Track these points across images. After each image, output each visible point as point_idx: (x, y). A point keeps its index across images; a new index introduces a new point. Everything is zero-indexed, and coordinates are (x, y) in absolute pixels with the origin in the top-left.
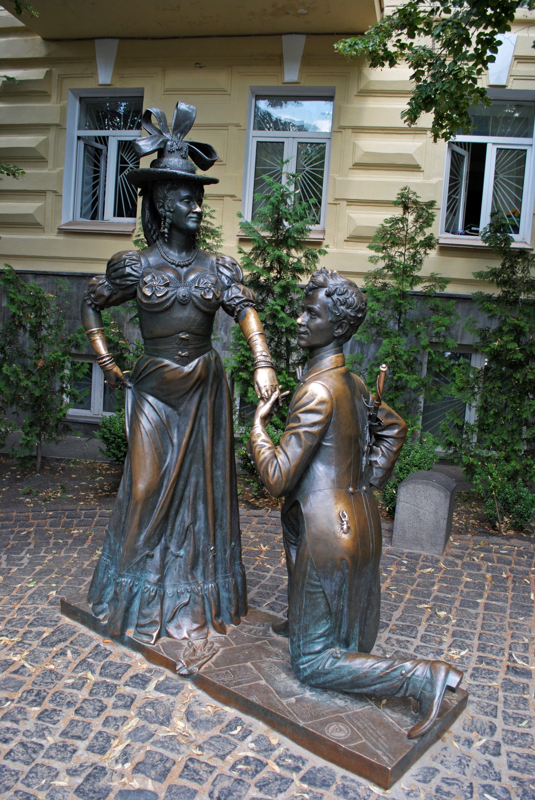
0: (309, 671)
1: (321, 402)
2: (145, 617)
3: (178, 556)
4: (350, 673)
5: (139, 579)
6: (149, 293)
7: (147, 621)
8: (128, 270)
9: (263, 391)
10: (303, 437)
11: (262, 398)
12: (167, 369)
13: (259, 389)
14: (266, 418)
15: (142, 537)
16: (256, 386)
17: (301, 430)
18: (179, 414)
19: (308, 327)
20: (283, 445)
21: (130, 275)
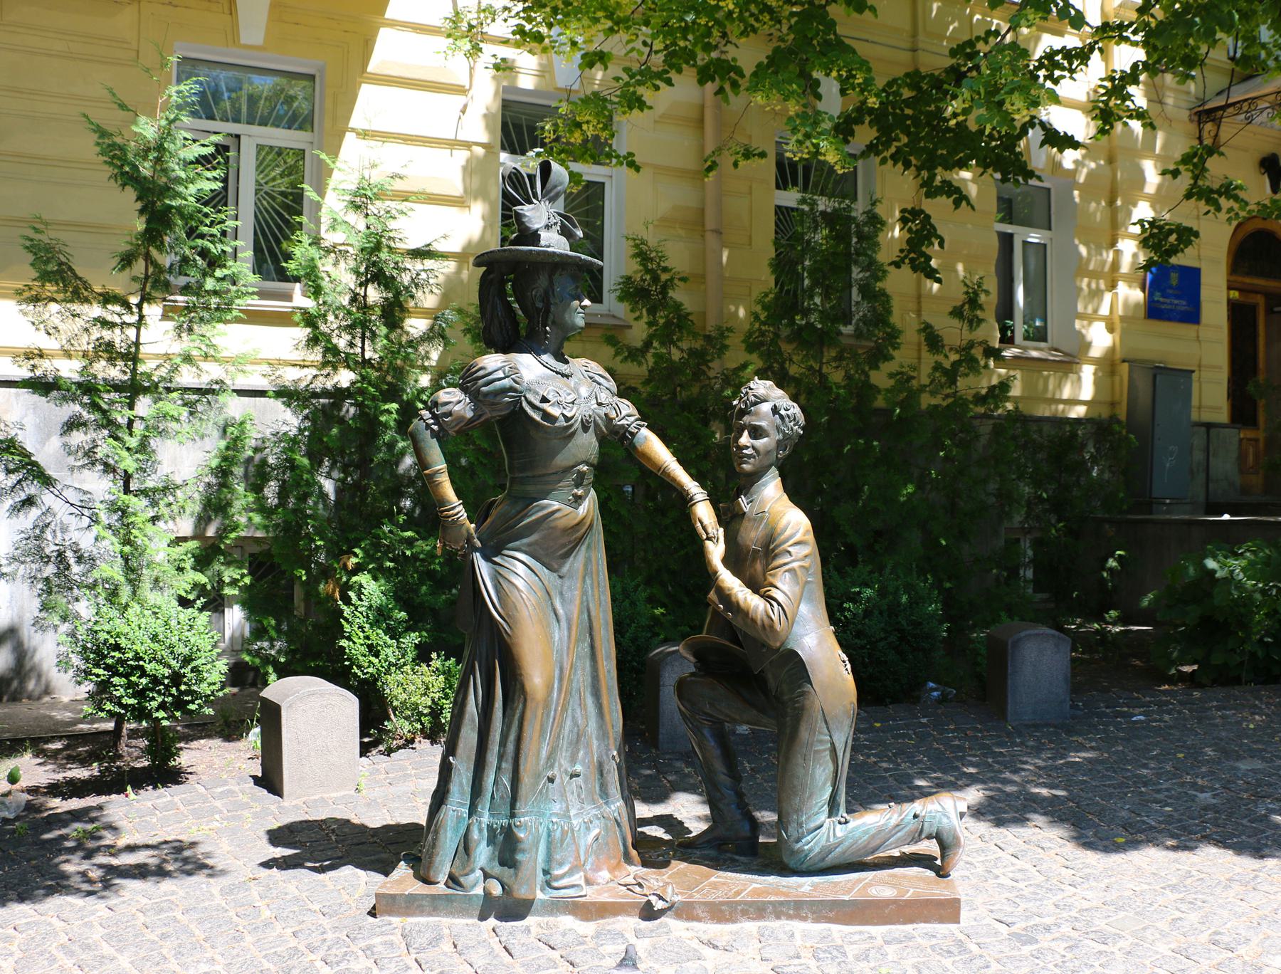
0: (817, 850)
1: (806, 532)
2: (561, 864)
3: (575, 775)
4: (865, 832)
5: (542, 815)
6: (555, 411)
7: (566, 868)
8: (507, 382)
9: (710, 530)
10: (799, 572)
11: (708, 539)
12: (557, 515)
13: (704, 528)
14: (726, 561)
15: (544, 754)
16: (699, 524)
17: (795, 565)
18: (560, 577)
19: (754, 448)
20: (779, 585)
21: (512, 389)
